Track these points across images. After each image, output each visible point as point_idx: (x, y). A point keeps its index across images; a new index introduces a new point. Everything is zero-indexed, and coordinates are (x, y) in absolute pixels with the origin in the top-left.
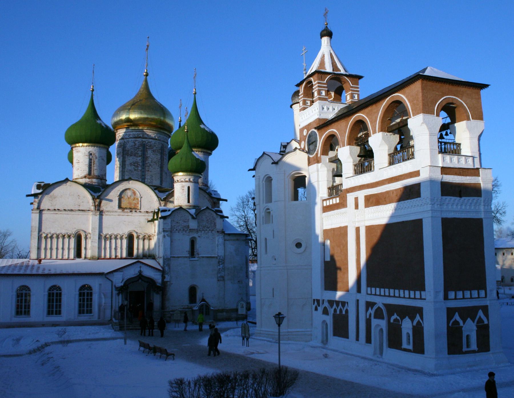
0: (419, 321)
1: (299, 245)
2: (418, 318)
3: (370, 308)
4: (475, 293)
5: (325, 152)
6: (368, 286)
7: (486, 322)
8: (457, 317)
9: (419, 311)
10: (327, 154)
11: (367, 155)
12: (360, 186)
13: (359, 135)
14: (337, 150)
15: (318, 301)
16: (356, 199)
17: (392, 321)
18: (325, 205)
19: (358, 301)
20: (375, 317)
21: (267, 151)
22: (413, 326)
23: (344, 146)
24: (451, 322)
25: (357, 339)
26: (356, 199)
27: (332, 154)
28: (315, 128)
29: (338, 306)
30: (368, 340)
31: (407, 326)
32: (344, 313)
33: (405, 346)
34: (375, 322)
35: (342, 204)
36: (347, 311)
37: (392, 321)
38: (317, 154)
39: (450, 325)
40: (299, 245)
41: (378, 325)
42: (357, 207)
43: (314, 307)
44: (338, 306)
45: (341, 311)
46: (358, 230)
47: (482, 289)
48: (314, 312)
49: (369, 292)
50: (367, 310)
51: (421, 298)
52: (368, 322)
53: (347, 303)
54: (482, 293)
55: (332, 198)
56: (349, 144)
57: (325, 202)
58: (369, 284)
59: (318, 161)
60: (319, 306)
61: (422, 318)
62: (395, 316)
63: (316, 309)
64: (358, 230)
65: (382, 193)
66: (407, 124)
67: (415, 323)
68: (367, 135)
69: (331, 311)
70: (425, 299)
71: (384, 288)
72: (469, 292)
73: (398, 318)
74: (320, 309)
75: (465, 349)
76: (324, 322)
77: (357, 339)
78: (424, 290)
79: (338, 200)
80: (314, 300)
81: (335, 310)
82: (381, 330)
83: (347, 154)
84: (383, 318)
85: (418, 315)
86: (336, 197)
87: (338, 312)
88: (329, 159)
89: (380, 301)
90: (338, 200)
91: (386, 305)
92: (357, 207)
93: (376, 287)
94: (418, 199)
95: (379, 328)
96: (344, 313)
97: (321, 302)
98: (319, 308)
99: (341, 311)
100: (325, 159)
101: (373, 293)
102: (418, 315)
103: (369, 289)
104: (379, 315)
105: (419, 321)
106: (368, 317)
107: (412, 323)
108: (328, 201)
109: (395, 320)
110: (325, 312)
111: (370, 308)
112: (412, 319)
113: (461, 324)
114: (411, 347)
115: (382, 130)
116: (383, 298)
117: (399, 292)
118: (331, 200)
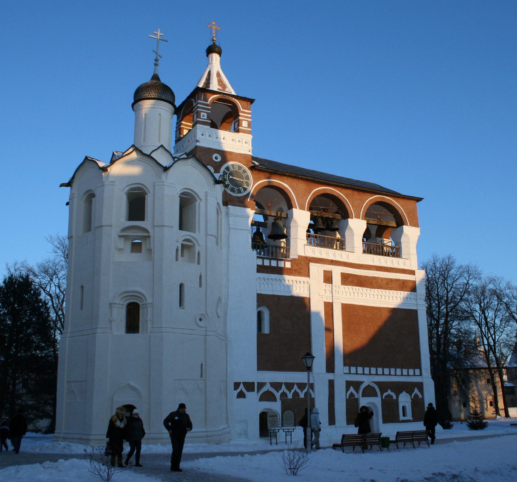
2: (416, 391)
4: (411, 372)
6: (345, 365)
22: (411, 399)
33: (402, 418)
37: (384, 398)
45: (296, 394)
47: (417, 368)
49: (347, 371)
54: (417, 372)
65: (366, 277)
72: (406, 370)
85: (416, 389)
89: (367, 380)
91: (378, 383)
93: (356, 366)
98: (247, 394)
102: (416, 389)
113: (395, 397)
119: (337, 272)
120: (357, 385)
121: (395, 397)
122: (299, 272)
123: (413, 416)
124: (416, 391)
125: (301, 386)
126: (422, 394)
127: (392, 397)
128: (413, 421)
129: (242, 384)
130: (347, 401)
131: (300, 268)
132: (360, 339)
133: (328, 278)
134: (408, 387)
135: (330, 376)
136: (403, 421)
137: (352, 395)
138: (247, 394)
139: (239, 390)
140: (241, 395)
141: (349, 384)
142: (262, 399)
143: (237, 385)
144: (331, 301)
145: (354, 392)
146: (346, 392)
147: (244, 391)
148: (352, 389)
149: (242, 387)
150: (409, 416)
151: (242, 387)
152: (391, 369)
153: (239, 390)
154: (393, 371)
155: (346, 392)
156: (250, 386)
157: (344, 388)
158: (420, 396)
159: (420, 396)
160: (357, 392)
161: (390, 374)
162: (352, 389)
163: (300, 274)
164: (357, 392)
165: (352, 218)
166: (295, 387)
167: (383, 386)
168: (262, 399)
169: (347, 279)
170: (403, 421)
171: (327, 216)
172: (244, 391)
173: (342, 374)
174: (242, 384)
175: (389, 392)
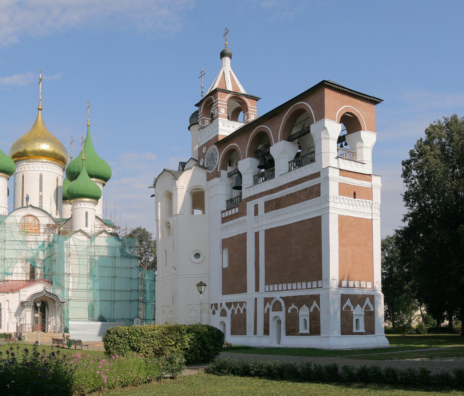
0: (316, 307)
1: (197, 255)
2: (315, 304)
3: (268, 303)
5: (224, 167)
6: (266, 284)
7: (372, 309)
8: (348, 303)
9: (317, 298)
10: (226, 170)
11: (267, 165)
12: (260, 194)
13: (259, 148)
14: (236, 164)
15: (216, 305)
16: (256, 206)
17: (289, 311)
18: (224, 216)
19: (256, 299)
20: (273, 310)
21: (167, 168)
22: (310, 313)
23: (244, 158)
24: (344, 306)
25: (255, 333)
26: (256, 206)
27: (230, 169)
28: (216, 144)
29: (235, 306)
30: (266, 332)
31: (304, 313)
32: (242, 312)
33: (302, 331)
34: (272, 314)
35: (243, 213)
36: (245, 310)
37: (289, 311)
38: (217, 169)
39: (343, 309)
40: (197, 255)
41: (276, 317)
42: (256, 213)
43: (211, 311)
44: (235, 306)
45: (239, 310)
46: (257, 234)
49: (267, 290)
50: (265, 305)
51: (318, 287)
52: (267, 316)
53: (245, 302)
55: (231, 209)
56: (249, 156)
57: (223, 214)
58: (268, 282)
59: (217, 175)
60: (217, 309)
61: (319, 304)
62: (293, 306)
63: (214, 313)
64: (257, 234)
66: (309, 132)
67: (311, 310)
68: (268, 146)
69: (229, 312)
70: (322, 287)
71: (282, 283)
73: (296, 308)
74: (218, 312)
75: (355, 330)
76: (222, 322)
77: (255, 333)
78: (321, 279)
79: (237, 210)
80: (212, 305)
81: (233, 311)
82: (279, 322)
83: (247, 166)
84: (281, 310)
86: (235, 208)
87: (236, 312)
88: (228, 174)
89: (277, 296)
90: (237, 210)
92: (256, 213)
93: (273, 284)
95: (277, 319)
96: (242, 312)
97: (219, 305)
99: (239, 310)
100: (224, 173)
101: (271, 289)
102: (315, 301)
103: (267, 287)
104: (277, 307)
105: (316, 307)
106: (266, 312)
108: (227, 212)
109: (292, 310)
110: (223, 313)
111: (268, 303)
112: (309, 306)
113: (352, 310)
114: (307, 331)
115: (283, 138)
116: (281, 292)
117: (297, 284)
118: (230, 211)
119: (261, 202)
123: (310, 330)
125: (241, 304)
135: (256, 295)
136: (302, 335)
146: (264, 308)
149: (213, 307)
152: (308, 283)
153: (213, 309)
154: (289, 286)
155: (264, 308)
157: (263, 304)
162: (268, 305)
169: (269, 206)
170: (302, 335)
175: (293, 306)
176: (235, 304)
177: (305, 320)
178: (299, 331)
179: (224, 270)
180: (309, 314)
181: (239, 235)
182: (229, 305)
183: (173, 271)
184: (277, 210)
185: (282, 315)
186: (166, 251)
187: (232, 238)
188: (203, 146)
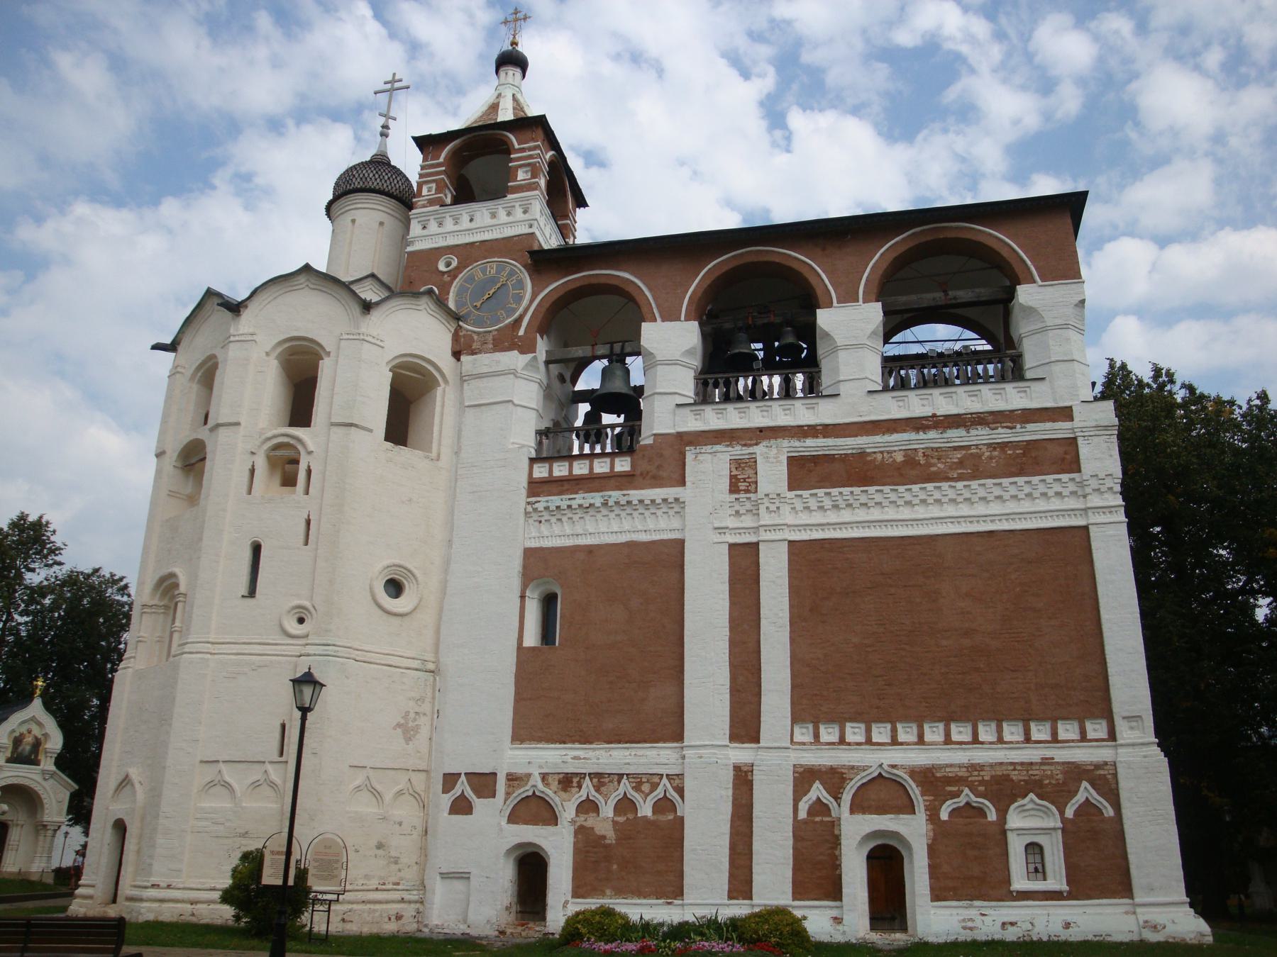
2: (1085, 792)
6: (796, 719)
12: (761, 430)
17: (944, 816)
32: (646, 810)
37: (944, 816)
45: (626, 805)
48: (446, 822)
67: (1069, 813)
69: (567, 809)
84: (911, 809)
90: (623, 465)
91: (915, 773)
93: (840, 720)
94: (1065, 477)
96: (646, 810)
98: (478, 803)
99: (626, 805)
102: (1085, 784)
107: (1062, 813)
120: (834, 778)
121: (992, 816)
122: (654, 477)
124: (1085, 792)
126: (1117, 806)
127: (981, 812)
128: (1071, 896)
129: (463, 778)
130: (798, 827)
131: (659, 467)
132: (855, 640)
133: (742, 481)
134: (1052, 786)
135: (742, 754)
137: (819, 808)
138: (478, 803)
139: (457, 791)
140: (461, 807)
141: (804, 778)
142: (513, 818)
143: (450, 780)
144: (785, 546)
145: (827, 798)
147: (469, 793)
148: (817, 791)
149: (462, 786)
150: (1056, 880)
151: (462, 786)
153: (457, 791)
156: (484, 783)
158: (1109, 812)
159: (1109, 812)
160: (837, 798)
161: (976, 740)
162: (817, 791)
163: (657, 481)
164: (837, 798)
165: (830, 305)
166: (625, 787)
167: (935, 782)
168: (513, 818)
171: (766, 321)
172: (469, 793)
173: (783, 748)
174: (463, 778)
176: (600, 779)
177: (1034, 849)
178: (1009, 882)
179: (523, 652)
180: (1059, 825)
181: (631, 545)
182: (567, 781)
183: (293, 627)
184: (857, 490)
185: (913, 830)
186: (257, 549)
187: (590, 550)
188: (438, 252)
